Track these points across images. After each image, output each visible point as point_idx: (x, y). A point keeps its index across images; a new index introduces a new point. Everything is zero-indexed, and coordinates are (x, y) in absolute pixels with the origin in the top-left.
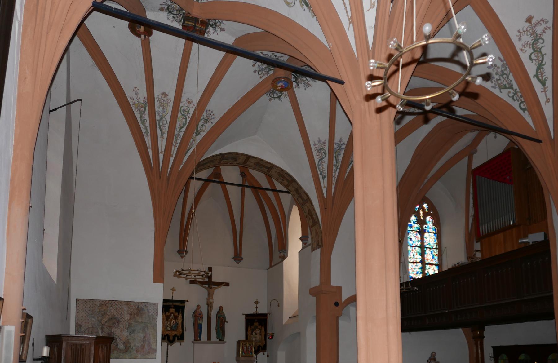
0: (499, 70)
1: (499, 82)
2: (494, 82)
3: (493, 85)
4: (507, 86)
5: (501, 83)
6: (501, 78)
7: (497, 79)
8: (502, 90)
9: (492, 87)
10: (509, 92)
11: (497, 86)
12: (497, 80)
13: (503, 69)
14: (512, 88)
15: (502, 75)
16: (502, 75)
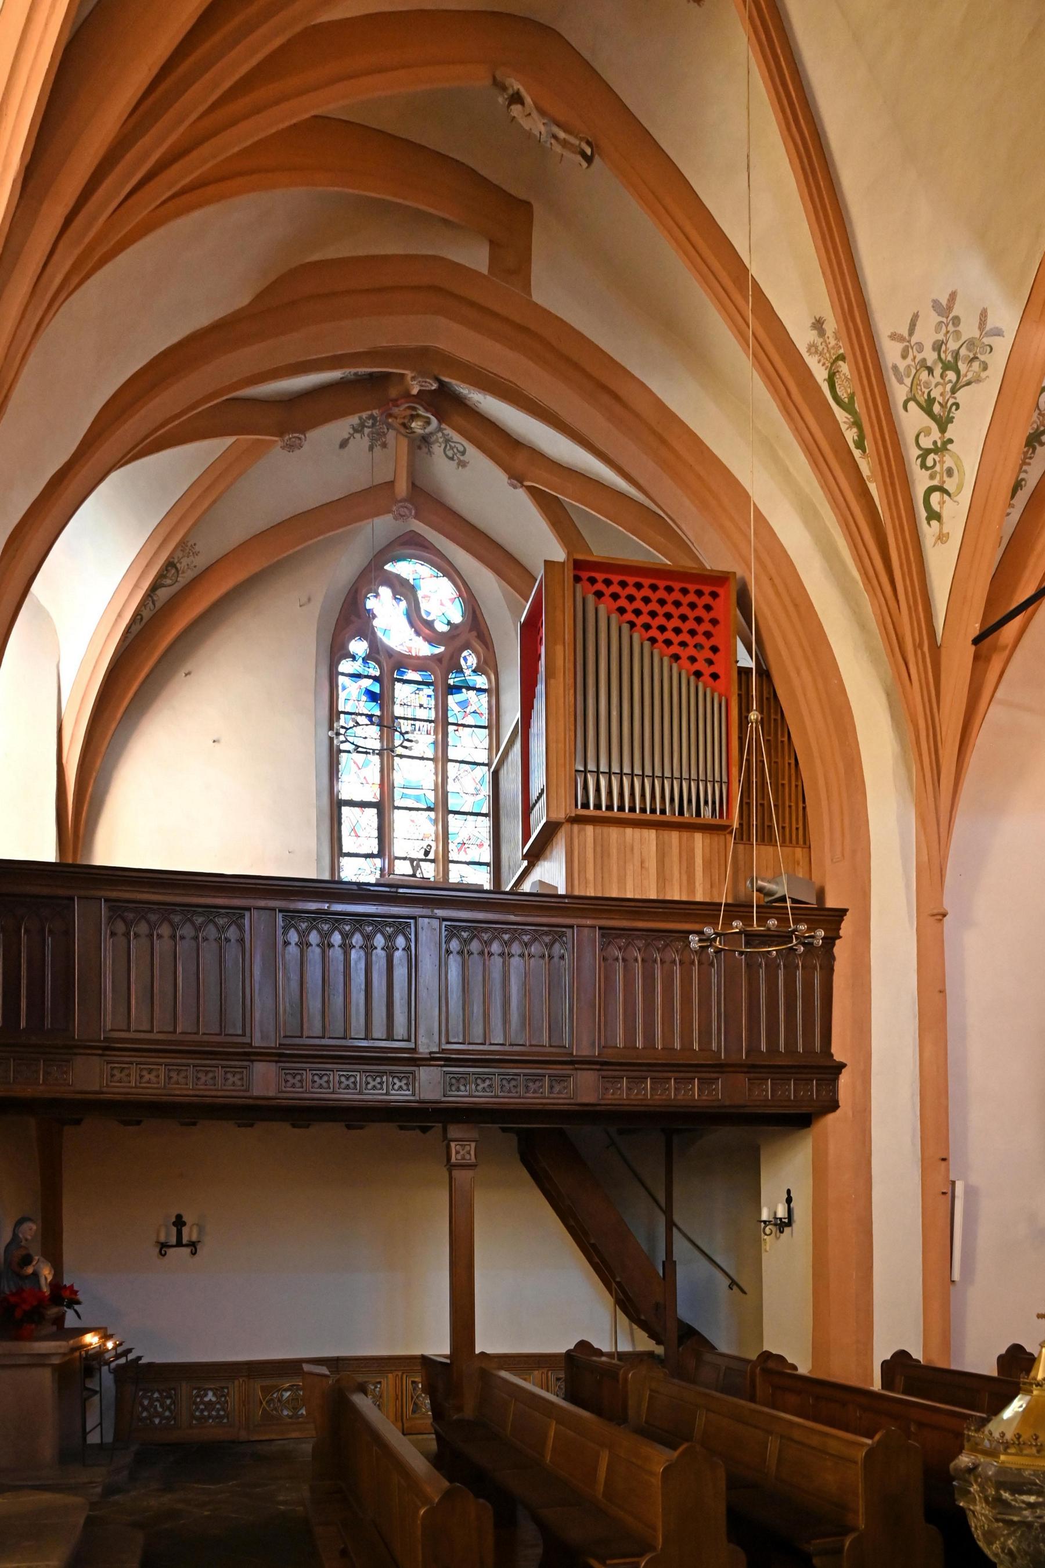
0: (953, 345)
1: (924, 375)
2: (909, 361)
3: (902, 365)
4: (936, 409)
5: (927, 384)
6: (938, 371)
7: (924, 360)
8: (912, 405)
9: (895, 368)
10: (928, 432)
11: (908, 381)
12: (923, 365)
13: (963, 352)
14: (943, 430)
15: (947, 367)
16: (947, 367)
